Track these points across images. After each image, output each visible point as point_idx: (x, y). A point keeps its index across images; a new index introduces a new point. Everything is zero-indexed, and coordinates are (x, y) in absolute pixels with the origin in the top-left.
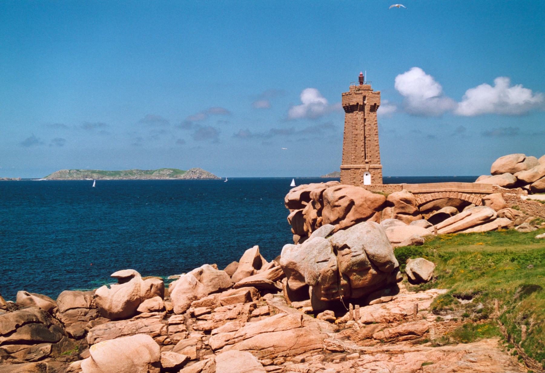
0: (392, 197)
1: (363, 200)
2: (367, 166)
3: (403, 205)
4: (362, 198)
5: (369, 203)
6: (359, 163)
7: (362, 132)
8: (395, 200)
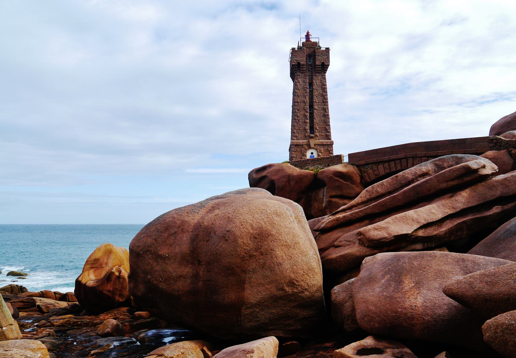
0: (322, 172)
1: (285, 180)
2: (312, 142)
3: (337, 184)
4: (284, 177)
5: (292, 183)
7: (307, 100)
8: (327, 176)
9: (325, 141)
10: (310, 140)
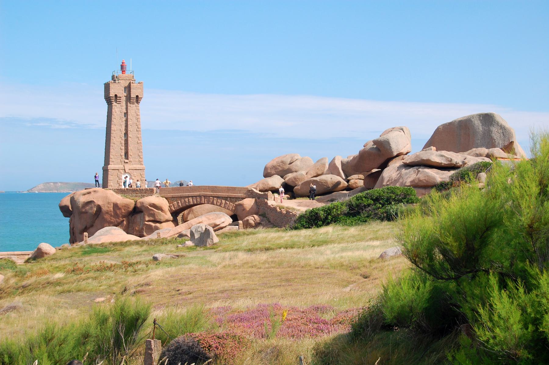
2: (127, 167)
6: (118, 164)
9: (138, 166)
10: (126, 165)
